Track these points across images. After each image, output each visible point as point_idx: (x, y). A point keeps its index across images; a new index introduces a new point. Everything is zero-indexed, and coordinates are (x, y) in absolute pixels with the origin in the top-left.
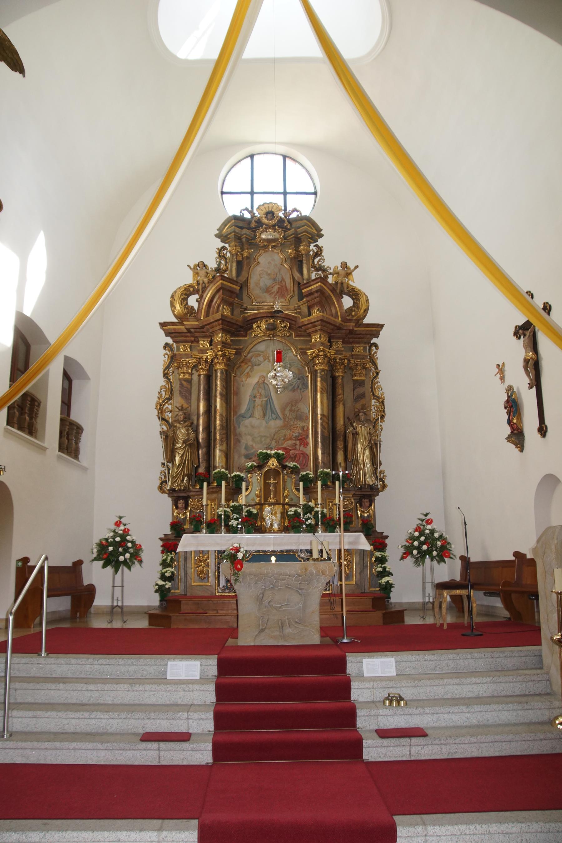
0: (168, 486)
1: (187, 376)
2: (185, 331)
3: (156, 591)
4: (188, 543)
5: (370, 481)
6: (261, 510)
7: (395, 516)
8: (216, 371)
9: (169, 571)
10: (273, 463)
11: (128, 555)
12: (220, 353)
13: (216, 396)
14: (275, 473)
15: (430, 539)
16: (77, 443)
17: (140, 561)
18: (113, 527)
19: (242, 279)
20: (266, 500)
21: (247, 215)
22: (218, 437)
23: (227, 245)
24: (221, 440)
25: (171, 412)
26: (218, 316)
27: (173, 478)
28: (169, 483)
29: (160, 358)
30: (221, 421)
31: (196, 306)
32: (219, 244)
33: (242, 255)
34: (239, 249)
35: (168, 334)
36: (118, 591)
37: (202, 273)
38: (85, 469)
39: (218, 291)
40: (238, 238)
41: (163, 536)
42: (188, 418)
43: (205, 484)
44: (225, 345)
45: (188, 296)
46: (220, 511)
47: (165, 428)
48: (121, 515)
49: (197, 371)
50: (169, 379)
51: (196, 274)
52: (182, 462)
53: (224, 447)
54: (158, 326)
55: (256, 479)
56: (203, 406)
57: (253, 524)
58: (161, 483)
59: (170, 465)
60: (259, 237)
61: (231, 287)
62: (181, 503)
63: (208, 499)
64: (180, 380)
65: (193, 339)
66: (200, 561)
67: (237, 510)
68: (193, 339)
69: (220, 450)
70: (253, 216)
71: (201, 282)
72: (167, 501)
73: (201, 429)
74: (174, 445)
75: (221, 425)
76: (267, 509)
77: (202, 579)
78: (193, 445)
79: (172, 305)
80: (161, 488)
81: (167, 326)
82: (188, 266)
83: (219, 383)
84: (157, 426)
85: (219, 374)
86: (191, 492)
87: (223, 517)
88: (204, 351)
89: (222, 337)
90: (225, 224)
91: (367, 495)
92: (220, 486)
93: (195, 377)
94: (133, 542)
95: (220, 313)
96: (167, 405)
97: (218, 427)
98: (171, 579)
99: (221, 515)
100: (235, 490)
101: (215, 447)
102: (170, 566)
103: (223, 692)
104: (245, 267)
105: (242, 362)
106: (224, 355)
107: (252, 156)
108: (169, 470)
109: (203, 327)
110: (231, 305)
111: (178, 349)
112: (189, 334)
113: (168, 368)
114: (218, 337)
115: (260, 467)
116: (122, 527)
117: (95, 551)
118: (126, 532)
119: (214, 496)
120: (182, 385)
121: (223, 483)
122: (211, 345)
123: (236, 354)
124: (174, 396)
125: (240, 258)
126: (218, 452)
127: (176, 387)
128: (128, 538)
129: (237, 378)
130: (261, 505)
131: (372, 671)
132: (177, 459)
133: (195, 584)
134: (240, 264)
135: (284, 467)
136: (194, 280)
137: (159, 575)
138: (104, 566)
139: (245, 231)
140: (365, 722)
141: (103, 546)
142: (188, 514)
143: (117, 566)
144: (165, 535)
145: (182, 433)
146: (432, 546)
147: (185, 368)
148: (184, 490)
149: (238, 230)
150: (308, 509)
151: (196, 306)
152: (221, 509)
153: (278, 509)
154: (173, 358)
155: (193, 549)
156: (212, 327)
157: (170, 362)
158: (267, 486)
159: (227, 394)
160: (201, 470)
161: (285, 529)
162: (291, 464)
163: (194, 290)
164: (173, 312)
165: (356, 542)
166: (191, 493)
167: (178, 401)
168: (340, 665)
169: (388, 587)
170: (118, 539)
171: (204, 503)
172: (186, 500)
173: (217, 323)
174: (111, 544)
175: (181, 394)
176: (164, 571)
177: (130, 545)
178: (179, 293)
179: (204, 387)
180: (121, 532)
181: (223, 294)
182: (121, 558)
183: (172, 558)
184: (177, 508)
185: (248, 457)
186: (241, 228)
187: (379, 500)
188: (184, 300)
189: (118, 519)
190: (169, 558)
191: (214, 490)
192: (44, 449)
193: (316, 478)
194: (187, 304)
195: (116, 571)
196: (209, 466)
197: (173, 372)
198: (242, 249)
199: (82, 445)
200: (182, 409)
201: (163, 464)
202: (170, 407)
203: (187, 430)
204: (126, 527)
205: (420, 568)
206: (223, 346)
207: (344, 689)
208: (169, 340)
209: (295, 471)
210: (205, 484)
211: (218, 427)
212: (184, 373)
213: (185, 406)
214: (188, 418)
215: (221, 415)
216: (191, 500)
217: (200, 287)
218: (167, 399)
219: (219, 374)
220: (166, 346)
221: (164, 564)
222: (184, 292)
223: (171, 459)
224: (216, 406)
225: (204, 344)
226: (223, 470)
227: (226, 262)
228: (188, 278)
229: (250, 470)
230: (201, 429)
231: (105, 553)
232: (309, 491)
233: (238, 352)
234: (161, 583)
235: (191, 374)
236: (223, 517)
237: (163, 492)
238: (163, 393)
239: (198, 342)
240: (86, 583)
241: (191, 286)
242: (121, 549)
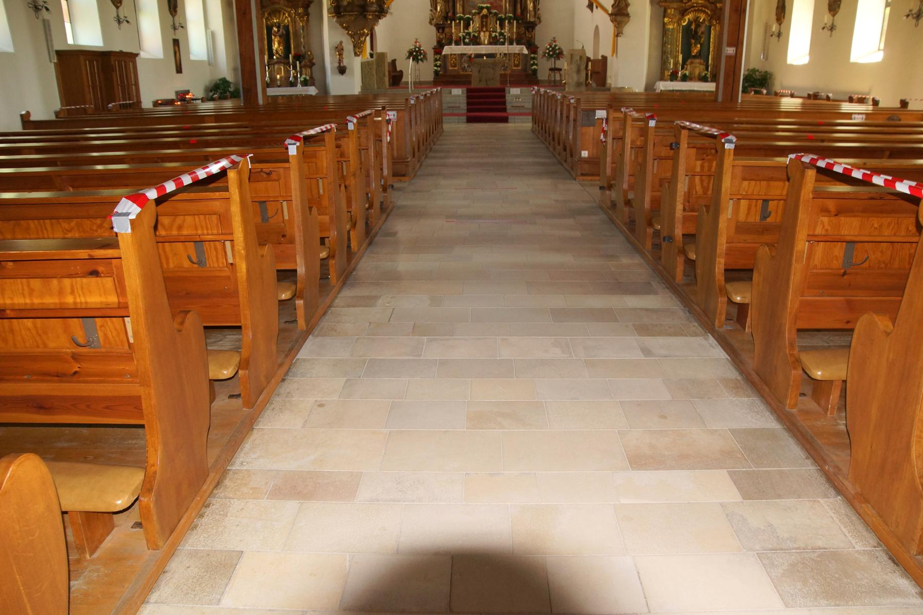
0: (434, 22)
4: (447, 50)
5: (532, 20)
6: (479, 34)
7: (543, 37)
9: (438, 63)
10: (485, 12)
14: (486, 16)
15: (554, 49)
20: (482, 28)
46: (460, 35)
55: (477, 19)
57: (476, 41)
67: (469, 34)
72: (434, 29)
76: (482, 34)
80: (430, 23)
91: (531, 26)
100: (467, 26)
103: (468, 97)
115: (479, 13)
130: (479, 32)
131: (515, 91)
132: (439, 8)
135: (490, 13)
140: (508, 106)
141: (411, 53)
146: (554, 53)
150: (501, 34)
153: (487, 34)
155: (449, 53)
158: (482, 22)
161: (490, 43)
162: (494, 11)
165: (522, 49)
168: (503, 90)
169: (535, 71)
172: (443, 29)
185: (474, 8)
187: (537, 28)
193: (505, 19)
196: (454, 13)
205: (549, 63)
207: (504, 97)
209: (496, 14)
221: (436, 60)
223: (436, 9)
229: (474, 14)
232: (502, 26)
240: (398, 69)
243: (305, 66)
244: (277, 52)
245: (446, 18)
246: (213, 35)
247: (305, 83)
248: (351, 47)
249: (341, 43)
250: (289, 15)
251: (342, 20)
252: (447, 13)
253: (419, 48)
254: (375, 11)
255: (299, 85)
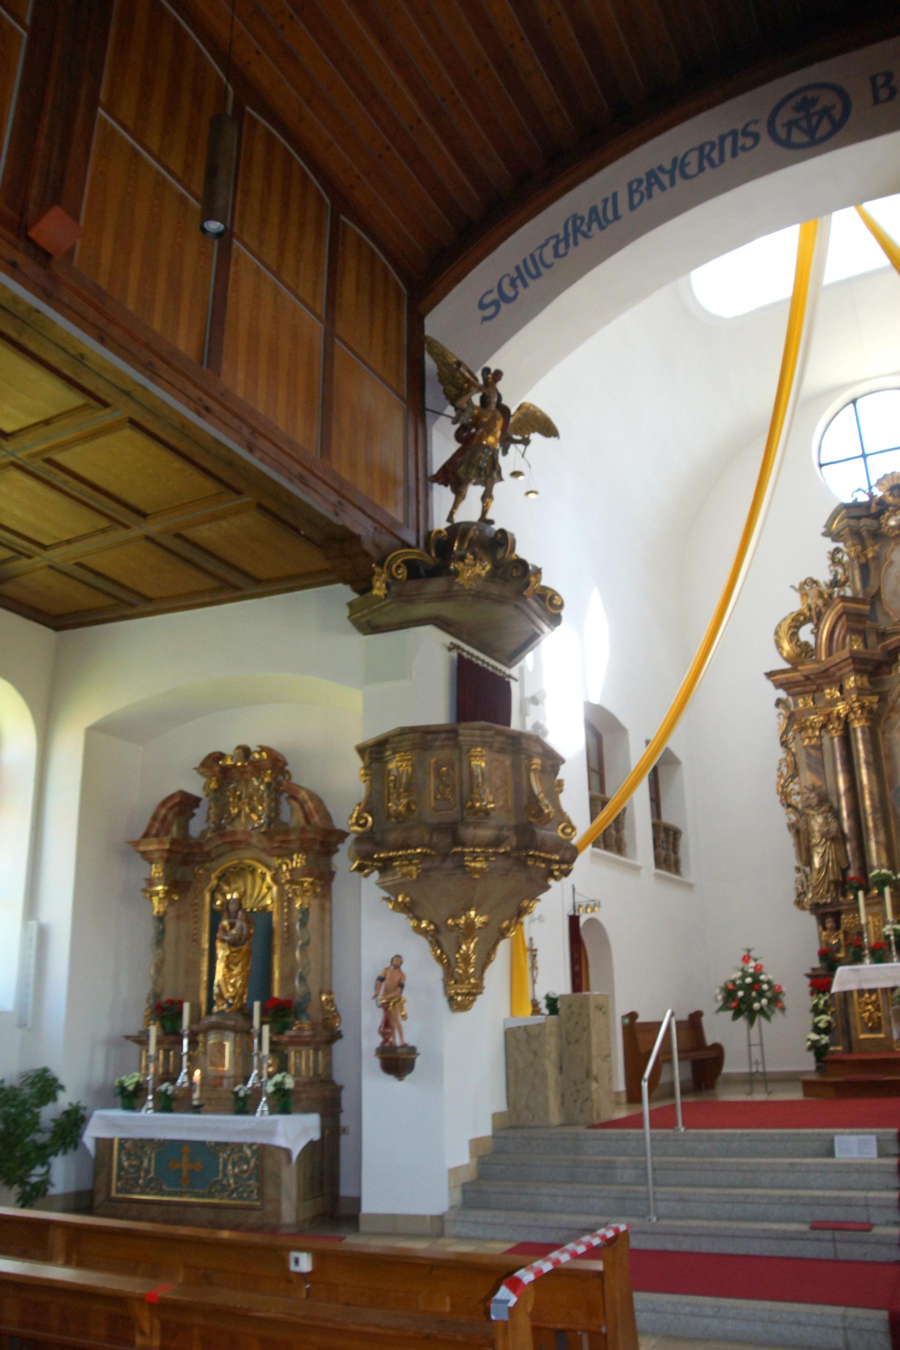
1: (814, 741)
2: (802, 678)
3: (810, 1049)
4: (846, 978)
8: (855, 729)
11: (764, 1001)
12: (856, 704)
13: (859, 766)
16: (675, 852)
17: (783, 1009)
18: (740, 964)
19: (872, 590)
21: (863, 498)
22: (871, 824)
23: (841, 545)
24: (875, 826)
25: (798, 794)
26: (845, 654)
27: (815, 888)
28: (810, 895)
29: (772, 721)
30: (872, 799)
31: (811, 640)
32: (829, 545)
33: (866, 555)
34: (859, 548)
35: (778, 685)
36: (756, 1051)
37: (813, 593)
38: (690, 886)
39: (839, 618)
40: (856, 534)
41: (809, 971)
42: (824, 801)
43: (861, 894)
44: (861, 691)
45: (798, 628)
46: (887, 930)
47: (793, 818)
48: (750, 947)
49: (829, 732)
50: (790, 749)
51: (805, 595)
52: (824, 865)
53: (882, 837)
54: (764, 678)
56: (845, 781)
58: (799, 895)
59: (808, 869)
60: (886, 525)
61: (858, 609)
62: (829, 923)
63: (867, 914)
64: (805, 747)
65: (814, 687)
66: (867, 1004)
68: (814, 687)
69: (877, 843)
70: (871, 496)
71: (813, 606)
72: (810, 921)
73: (845, 814)
74: (809, 841)
75: (873, 806)
77: (872, 1030)
78: (837, 839)
79: (779, 646)
80: (799, 903)
81: (775, 675)
82: (792, 587)
83: (861, 747)
84: (782, 818)
85: (859, 735)
86: (841, 904)
87: (892, 938)
88: (833, 703)
89: (855, 681)
90: (833, 518)
92: (881, 894)
93: (826, 741)
94: (769, 982)
95: (847, 648)
96: (791, 786)
97: (869, 810)
98: (826, 1031)
99: (889, 936)
101: (868, 840)
102: (823, 1012)
104: (873, 573)
105: (891, 710)
106: (862, 707)
107: (854, 402)
108: (807, 876)
109: (826, 671)
110: (863, 633)
111: (796, 705)
112: (808, 682)
113: (785, 732)
114: (851, 682)
116: (752, 964)
117: (720, 997)
118: (758, 970)
119: (876, 909)
120: (809, 755)
121: (887, 891)
122: (841, 693)
123: (880, 700)
124: (801, 771)
125: (863, 561)
126: (873, 846)
127: (802, 759)
128: (762, 977)
129: (886, 735)
132: (817, 861)
133: (862, 1036)
134: (865, 569)
136: (803, 604)
137: (810, 1026)
138: (735, 1017)
139: (864, 522)
141: (729, 993)
142: (841, 936)
143: (751, 1017)
144: (814, 969)
145: (817, 822)
147: (810, 731)
148: (831, 903)
149: (853, 522)
151: (811, 640)
152: (888, 927)
154: (791, 718)
155: (853, 986)
156: (840, 669)
157: (788, 725)
159: (875, 760)
160: (852, 873)
163: (805, 619)
164: (781, 654)
166: (842, 908)
167: (807, 778)
170: (749, 980)
171: (863, 921)
172: (837, 916)
173: (844, 663)
174: (741, 987)
175: (809, 767)
176: (817, 1019)
177: (765, 987)
178: (785, 627)
179: (841, 755)
180: (751, 970)
181: (848, 620)
182: (756, 1006)
183: (826, 1002)
184: (825, 929)
186: (858, 518)
188: (793, 635)
189: (745, 953)
190: (822, 1002)
191: (876, 900)
192: (637, 869)
194: (798, 640)
195: (751, 1022)
196: (864, 867)
197: (794, 738)
198: (864, 548)
199: (681, 853)
200: (813, 789)
201: (798, 870)
202: (797, 787)
203: (826, 818)
204: (759, 962)
206: (859, 695)
208: (782, 694)
210: (861, 894)
211: (869, 810)
212: (810, 738)
213: (818, 783)
214: (824, 801)
215: (871, 793)
216: (843, 916)
217: (813, 613)
218: (790, 776)
219: (859, 735)
220: (779, 702)
221: (816, 1011)
222: (793, 624)
223: (809, 862)
224: (861, 782)
225: (830, 692)
226: (884, 871)
227: (845, 570)
228: (795, 604)
230: (845, 814)
231: (734, 1000)
233: (883, 698)
234: (814, 1037)
235: (820, 737)
236: (892, 938)
237: (803, 908)
238: (785, 770)
239: (823, 690)
240: (710, 1040)
241: (800, 613)
242: (754, 994)
243: (297, 1042)
244: (221, 995)
245: (842, 885)
246: (43, 937)
247: (283, 1102)
248: (437, 973)
249: (397, 963)
250: (275, 879)
251: (389, 879)
252: (844, 871)
253: (755, 976)
254: (497, 842)
255: (263, 1106)
